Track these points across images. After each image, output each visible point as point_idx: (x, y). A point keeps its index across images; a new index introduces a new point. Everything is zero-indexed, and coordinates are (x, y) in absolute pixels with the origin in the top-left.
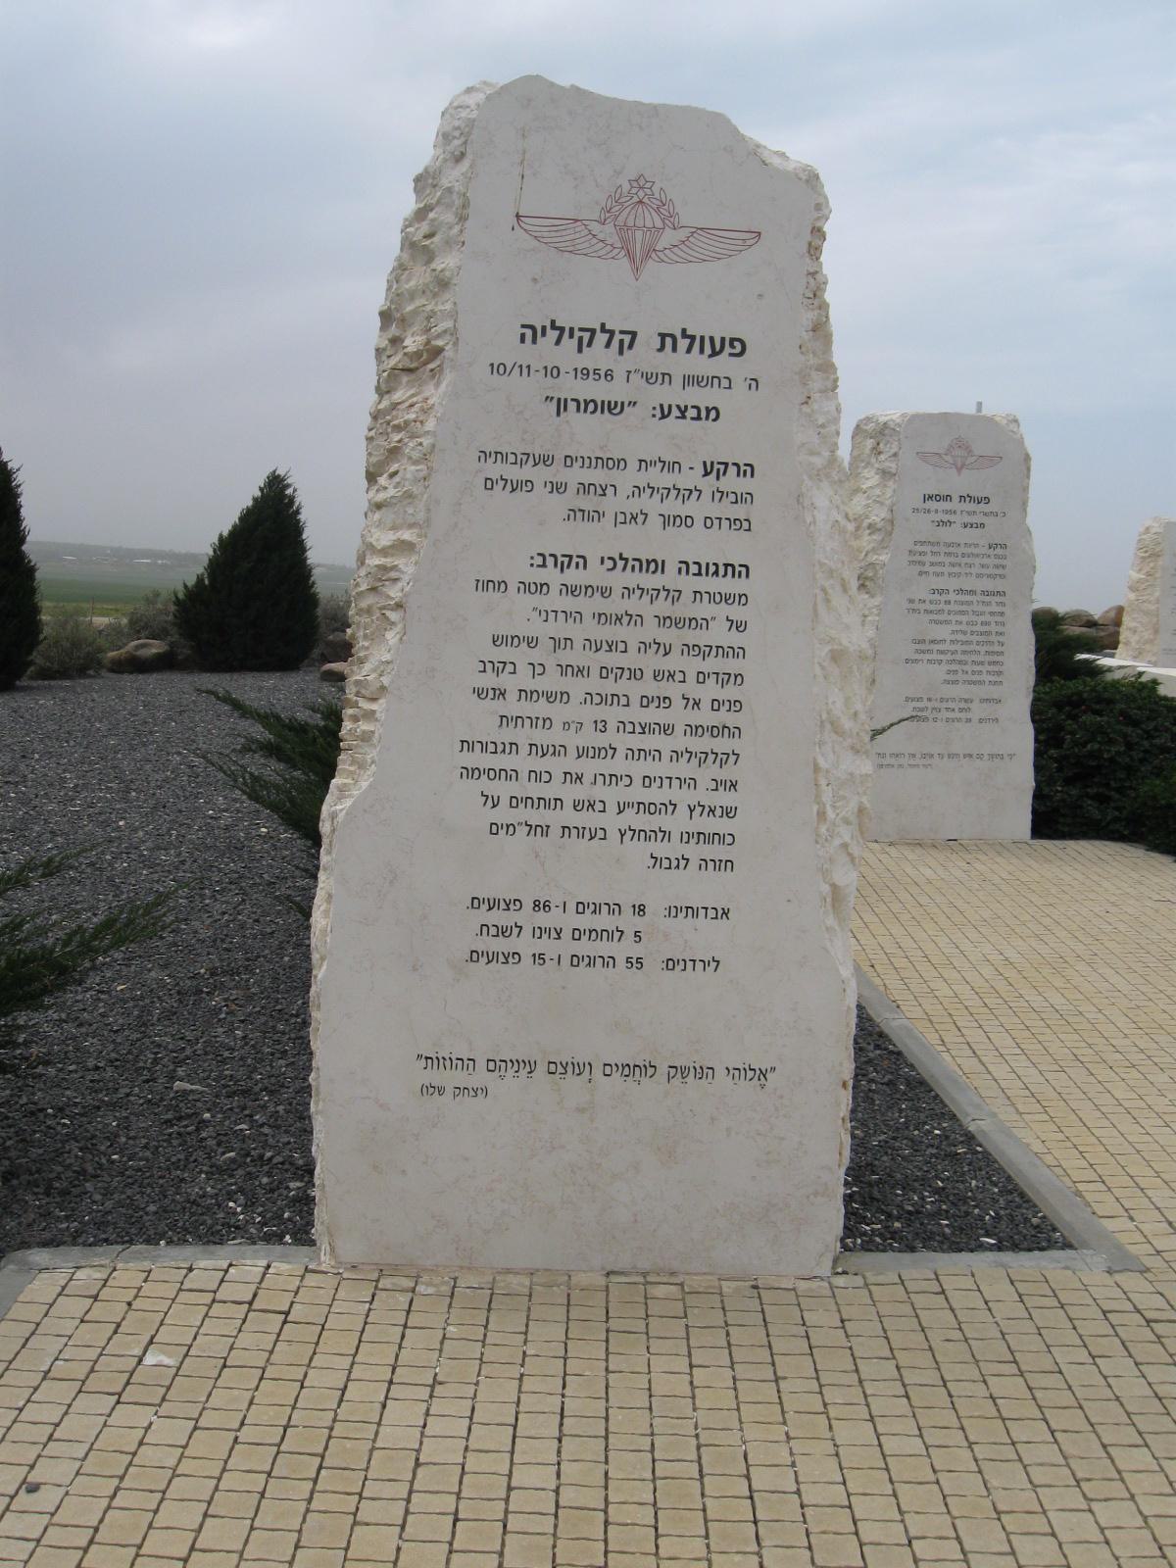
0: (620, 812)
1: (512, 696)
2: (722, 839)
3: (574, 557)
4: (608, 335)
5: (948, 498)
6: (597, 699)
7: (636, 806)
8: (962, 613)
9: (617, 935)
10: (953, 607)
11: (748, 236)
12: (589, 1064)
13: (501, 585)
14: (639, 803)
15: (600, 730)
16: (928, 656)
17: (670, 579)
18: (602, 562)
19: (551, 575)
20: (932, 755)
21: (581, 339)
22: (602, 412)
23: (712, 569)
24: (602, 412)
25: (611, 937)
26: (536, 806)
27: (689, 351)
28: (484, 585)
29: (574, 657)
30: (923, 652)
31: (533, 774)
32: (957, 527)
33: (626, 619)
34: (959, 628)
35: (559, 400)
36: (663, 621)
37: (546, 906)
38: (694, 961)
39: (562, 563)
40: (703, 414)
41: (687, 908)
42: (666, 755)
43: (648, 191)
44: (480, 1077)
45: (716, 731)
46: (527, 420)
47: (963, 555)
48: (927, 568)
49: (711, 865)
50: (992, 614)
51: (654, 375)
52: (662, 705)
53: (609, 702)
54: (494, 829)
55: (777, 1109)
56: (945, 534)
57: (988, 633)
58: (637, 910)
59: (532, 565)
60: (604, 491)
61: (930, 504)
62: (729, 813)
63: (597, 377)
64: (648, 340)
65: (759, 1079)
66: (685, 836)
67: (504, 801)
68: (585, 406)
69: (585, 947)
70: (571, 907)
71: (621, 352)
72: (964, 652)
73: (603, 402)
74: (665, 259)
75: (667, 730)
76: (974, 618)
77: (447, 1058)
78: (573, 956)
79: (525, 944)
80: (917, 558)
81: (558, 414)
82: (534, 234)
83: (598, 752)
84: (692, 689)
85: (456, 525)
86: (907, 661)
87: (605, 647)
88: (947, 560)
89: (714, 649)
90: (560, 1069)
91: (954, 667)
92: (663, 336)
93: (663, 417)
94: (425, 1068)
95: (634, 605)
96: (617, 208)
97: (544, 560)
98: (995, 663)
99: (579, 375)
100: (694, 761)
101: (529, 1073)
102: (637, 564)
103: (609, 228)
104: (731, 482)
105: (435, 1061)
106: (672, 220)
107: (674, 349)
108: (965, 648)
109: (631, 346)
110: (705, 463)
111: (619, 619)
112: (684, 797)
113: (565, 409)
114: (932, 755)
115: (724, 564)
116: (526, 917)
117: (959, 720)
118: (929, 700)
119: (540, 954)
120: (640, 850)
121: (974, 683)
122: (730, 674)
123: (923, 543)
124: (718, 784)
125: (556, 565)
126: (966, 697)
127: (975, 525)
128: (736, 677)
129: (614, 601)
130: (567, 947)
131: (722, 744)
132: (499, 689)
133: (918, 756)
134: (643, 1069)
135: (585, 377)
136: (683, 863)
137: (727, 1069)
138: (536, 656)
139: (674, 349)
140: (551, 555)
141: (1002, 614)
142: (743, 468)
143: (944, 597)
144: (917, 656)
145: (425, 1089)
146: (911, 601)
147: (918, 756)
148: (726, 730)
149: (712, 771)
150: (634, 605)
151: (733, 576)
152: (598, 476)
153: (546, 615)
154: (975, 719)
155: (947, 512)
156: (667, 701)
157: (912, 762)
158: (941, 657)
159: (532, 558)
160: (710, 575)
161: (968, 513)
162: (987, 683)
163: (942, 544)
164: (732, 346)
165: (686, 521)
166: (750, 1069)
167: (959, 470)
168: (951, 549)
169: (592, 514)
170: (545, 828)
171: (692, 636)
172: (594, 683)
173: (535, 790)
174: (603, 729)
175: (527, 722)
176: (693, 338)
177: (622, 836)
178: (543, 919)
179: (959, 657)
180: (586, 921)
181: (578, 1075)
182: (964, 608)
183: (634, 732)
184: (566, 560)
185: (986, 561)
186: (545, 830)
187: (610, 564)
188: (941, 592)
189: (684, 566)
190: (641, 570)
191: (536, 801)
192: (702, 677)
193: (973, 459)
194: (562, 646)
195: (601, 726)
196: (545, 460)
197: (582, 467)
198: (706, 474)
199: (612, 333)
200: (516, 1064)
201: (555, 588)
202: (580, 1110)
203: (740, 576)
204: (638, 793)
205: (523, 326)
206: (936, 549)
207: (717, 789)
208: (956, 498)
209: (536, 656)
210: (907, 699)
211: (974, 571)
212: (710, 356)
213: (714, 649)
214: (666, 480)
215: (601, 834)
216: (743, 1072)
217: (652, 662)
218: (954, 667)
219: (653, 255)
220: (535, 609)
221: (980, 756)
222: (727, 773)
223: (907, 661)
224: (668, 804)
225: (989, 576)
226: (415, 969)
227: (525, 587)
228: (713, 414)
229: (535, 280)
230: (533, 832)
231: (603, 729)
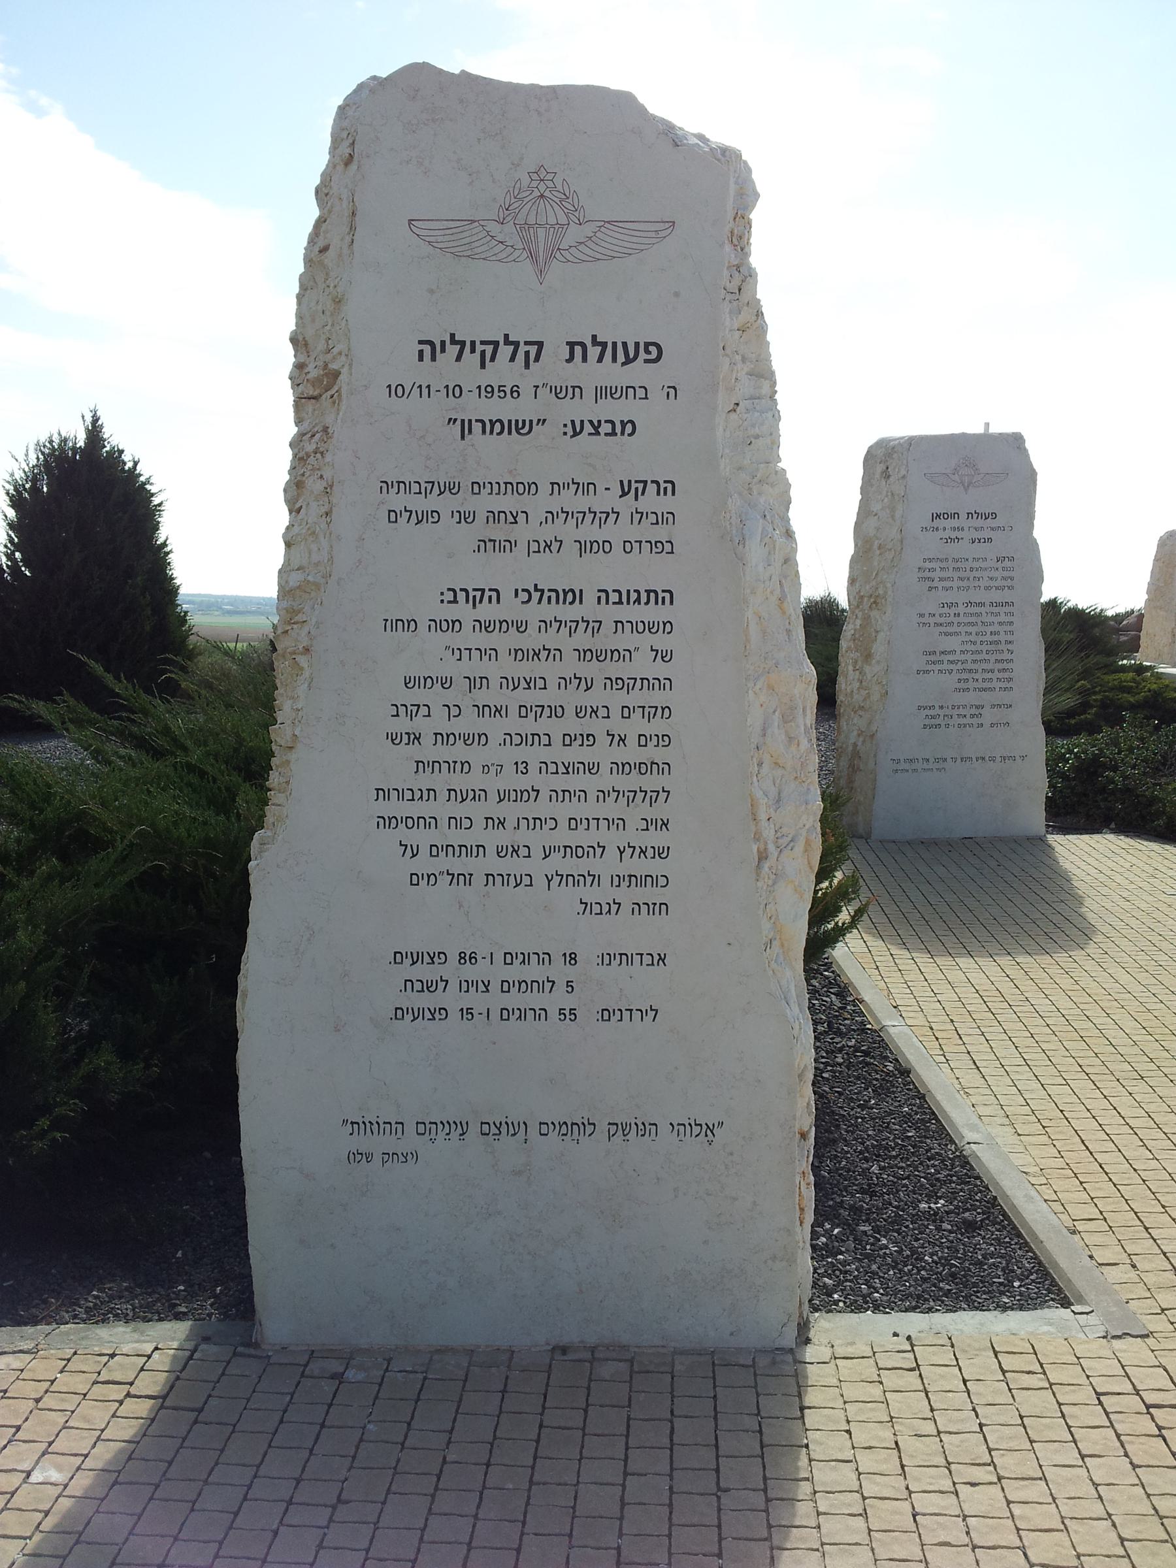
0: (546, 857)
1: (427, 740)
2: (655, 881)
4: (513, 347)
5: (955, 515)
6: (517, 739)
7: (562, 849)
9: (548, 986)
10: (962, 619)
11: (662, 226)
12: (524, 1123)
13: (410, 624)
14: (565, 847)
15: (522, 772)
16: (938, 667)
17: (588, 609)
18: (516, 595)
19: (463, 611)
20: (946, 759)
21: (483, 353)
22: (510, 433)
23: (634, 596)
24: (510, 433)
25: (541, 989)
26: (457, 853)
27: (600, 360)
28: (392, 624)
29: (491, 696)
30: (934, 663)
31: (453, 821)
33: (544, 654)
34: (968, 638)
35: (463, 421)
36: (583, 654)
37: (473, 958)
38: (631, 1010)
39: (474, 597)
40: (618, 429)
41: (621, 954)
42: (592, 797)
43: (550, 184)
44: (410, 1141)
45: (643, 768)
46: (430, 445)
47: (972, 569)
48: (935, 584)
49: (644, 908)
50: (1000, 623)
51: (564, 389)
52: (586, 742)
53: (530, 742)
54: (414, 879)
55: (726, 1167)
56: (954, 550)
57: (998, 642)
58: (568, 959)
59: (442, 601)
60: (515, 518)
61: (937, 523)
62: (661, 853)
63: (502, 394)
64: (556, 350)
65: (706, 1136)
66: (616, 879)
67: (424, 851)
68: (491, 426)
69: (515, 1000)
70: (498, 958)
71: (527, 366)
72: (974, 661)
73: (510, 421)
74: (571, 258)
75: (591, 769)
76: (983, 629)
77: (374, 1123)
78: (502, 1009)
79: (452, 999)
80: (927, 574)
81: (463, 437)
82: (427, 239)
83: (520, 795)
84: (617, 724)
85: (360, 561)
86: (918, 672)
87: (523, 684)
88: (956, 575)
89: (639, 682)
90: (494, 1130)
91: (965, 676)
92: (572, 345)
93: (575, 434)
94: (351, 1134)
95: (550, 639)
96: (516, 205)
97: (455, 596)
99: (483, 393)
100: (623, 801)
101: (461, 1135)
102: (553, 595)
103: (509, 227)
104: (650, 501)
105: (362, 1126)
106: (576, 214)
107: (585, 359)
109: (537, 359)
110: (621, 482)
111: (537, 654)
112: (612, 838)
113: (470, 431)
114: (946, 759)
115: (646, 591)
116: (451, 970)
117: (971, 725)
118: (941, 707)
119: (467, 1009)
120: (568, 896)
121: (984, 690)
122: (657, 708)
123: (930, 560)
124: (648, 824)
126: (977, 704)
127: (983, 540)
128: (663, 709)
129: (530, 636)
130: (496, 1000)
131: (652, 782)
132: (414, 734)
134: (582, 1127)
135: (489, 395)
136: (614, 908)
137: (671, 1124)
138: (451, 696)
139: (585, 359)
140: (461, 590)
142: (663, 486)
143: (953, 610)
144: (929, 667)
145: (352, 1156)
146: (922, 615)
147: (931, 760)
148: (655, 766)
149: (645, 810)
150: (550, 639)
151: (657, 603)
152: (507, 503)
153: (459, 653)
154: (987, 724)
155: (954, 529)
156: (591, 738)
157: (926, 766)
158: (951, 667)
160: (632, 603)
164: (648, 352)
165: (605, 546)
166: (696, 1125)
167: (966, 490)
168: (959, 565)
169: (503, 543)
170: (468, 877)
171: (614, 669)
172: (513, 723)
173: (456, 837)
174: (525, 771)
175: (445, 766)
176: (604, 345)
177: (549, 881)
178: (470, 972)
179: (969, 666)
180: (515, 972)
181: (512, 1135)
182: (973, 619)
183: (557, 773)
184: (478, 594)
186: (468, 879)
187: (525, 596)
188: (950, 605)
189: (603, 595)
190: (557, 602)
191: (457, 849)
192: (626, 712)
194: (478, 685)
195: (522, 767)
196: (451, 488)
197: (491, 493)
198: (624, 494)
199: (516, 344)
200: (447, 1126)
201: (468, 625)
202: (518, 1173)
203: (663, 603)
204: (563, 836)
205: (421, 342)
206: (944, 565)
207: (647, 829)
208: (963, 516)
209: (451, 696)
210: (920, 708)
211: (982, 583)
212: (623, 364)
213: (639, 682)
214: (582, 502)
215: (526, 880)
216: (688, 1127)
217: (572, 698)
218: (965, 676)
219: (558, 255)
220: (447, 648)
221: (993, 759)
222: (659, 811)
223: (918, 672)
224: (596, 846)
226: (337, 1030)
227: (436, 625)
228: (629, 428)
229: (431, 291)
230: (455, 880)
231: (525, 771)
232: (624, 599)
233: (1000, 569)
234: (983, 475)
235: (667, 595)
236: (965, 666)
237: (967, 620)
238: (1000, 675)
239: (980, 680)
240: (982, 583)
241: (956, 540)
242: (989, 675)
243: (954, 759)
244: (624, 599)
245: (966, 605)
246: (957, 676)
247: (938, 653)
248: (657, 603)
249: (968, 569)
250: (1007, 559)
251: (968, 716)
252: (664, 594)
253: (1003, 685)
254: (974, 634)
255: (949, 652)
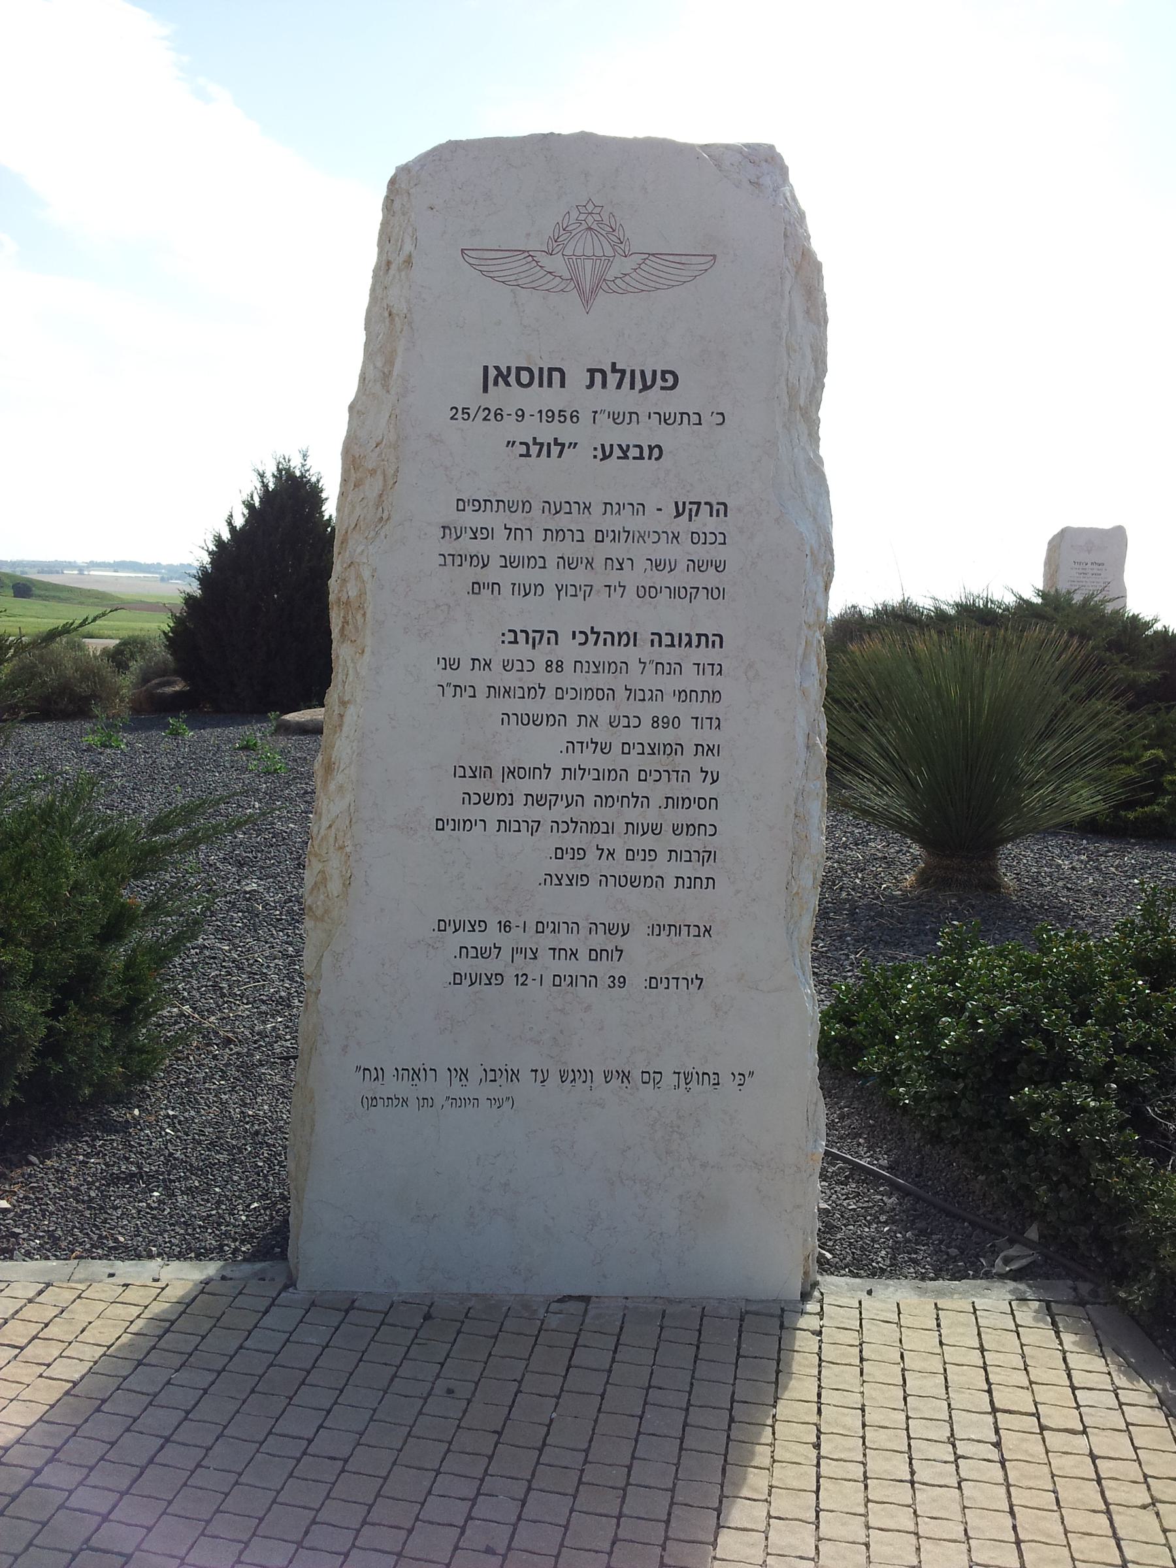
5: (554, 376)
8: (597, 693)
10: (570, 679)
16: (494, 812)
20: (516, 1074)
30: (485, 800)
32: (581, 459)
34: (585, 734)
47: (600, 536)
48: (493, 573)
50: (683, 695)
61: (499, 396)
72: (604, 800)
76: (633, 708)
80: (467, 545)
86: (440, 824)
88: (553, 550)
91: (574, 840)
98: (693, 828)
108: (607, 788)
114: (516, 1074)
117: (591, 980)
118: (505, 926)
121: (632, 882)
123: (480, 505)
133: (475, 1074)
141: (714, 695)
143: (542, 654)
146: (451, 664)
147: (475, 1074)
154: (637, 981)
155: (550, 416)
157: (458, 1090)
158: (536, 812)
161: (614, 417)
162: (670, 882)
163: (537, 506)
167: (587, 299)
168: (563, 521)
179: (589, 812)
182: (602, 680)
185: (666, 550)
188: (535, 638)
193: (629, 264)
206: (517, 520)
208: (577, 377)
210: (442, 925)
211: (632, 578)
218: (574, 840)
221: (653, 1077)
223: (440, 824)
225: (674, 593)
233: (685, 538)
234: (638, 258)
236: (575, 812)
237: (581, 681)
238: (681, 842)
239: (620, 854)
240: (632, 578)
241: (555, 450)
242: (649, 841)
243: (539, 1073)
245: (582, 638)
246: (549, 840)
247: (498, 774)
249: (589, 536)
250: (705, 509)
251: (583, 954)
253: (686, 870)
254: (603, 721)
255: (532, 772)
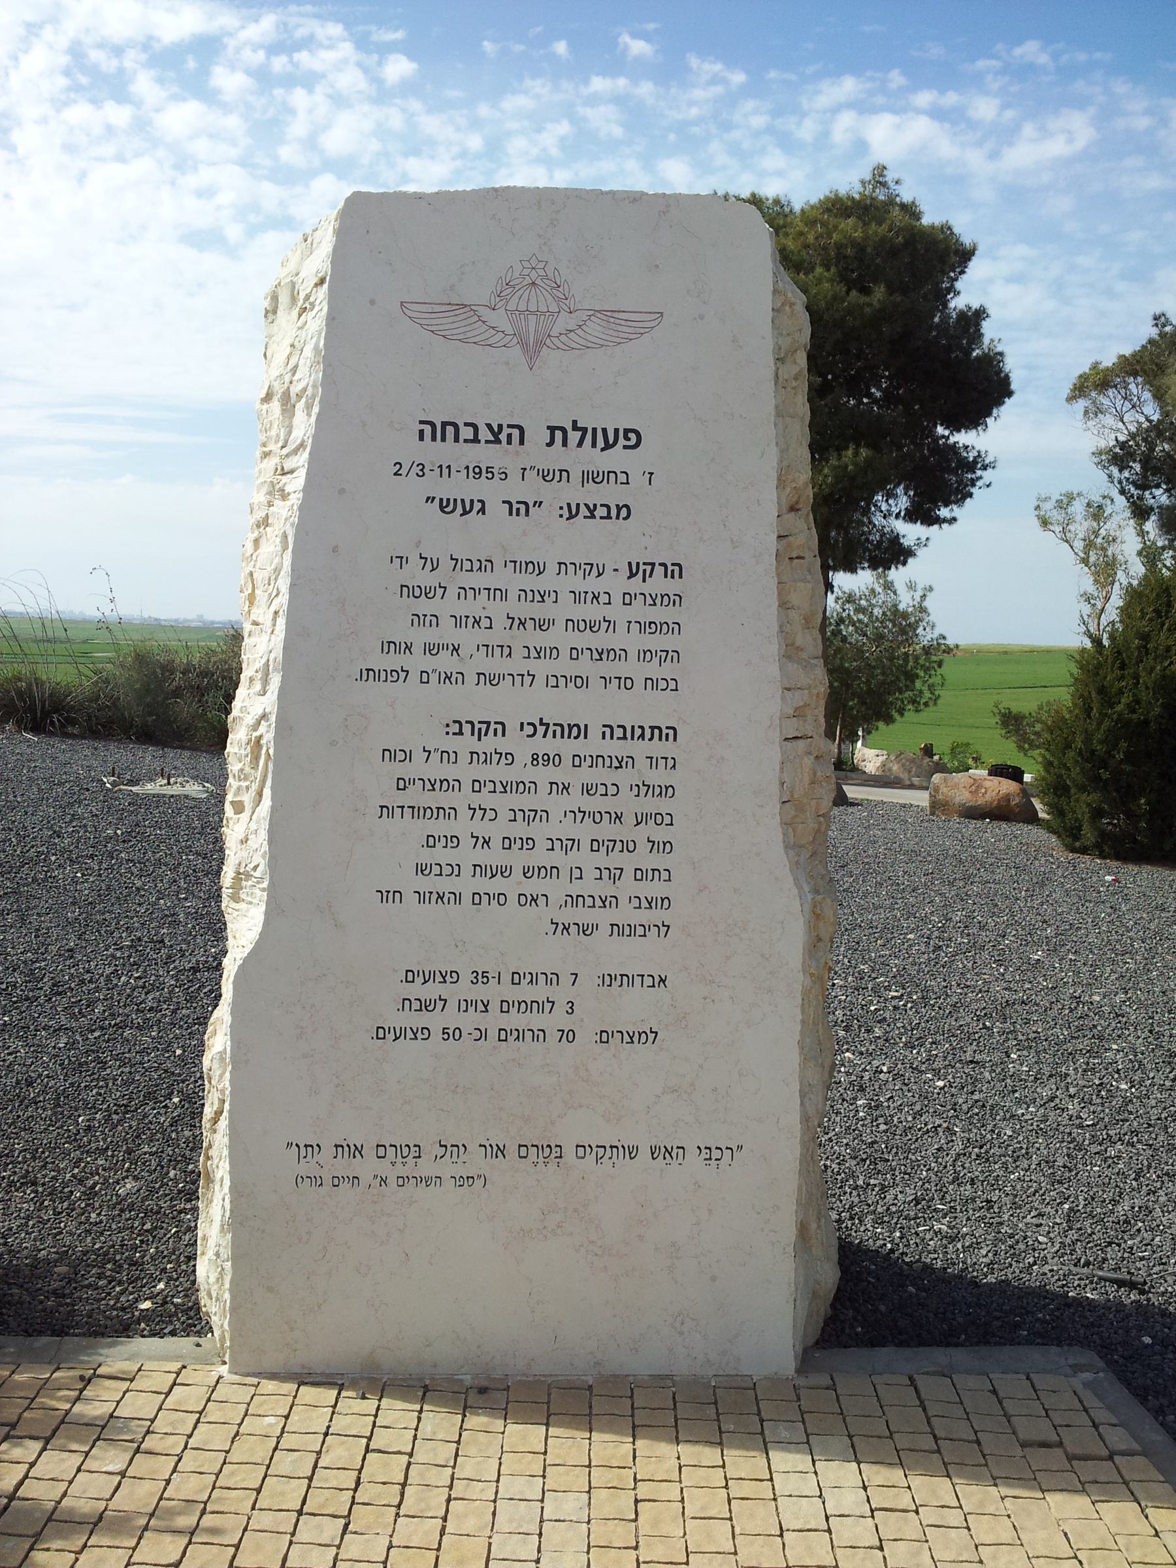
3: (492, 723)
18: (522, 729)
23: (638, 732)
27: (580, 444)
39: (480, 729)
51: (551, 472)
59: (447, 733)
102: (558, 729)
115: (650, 727)
125: (473, 734)
151: (660, 739)
159: (448, 725)
164: (627, 438)
184: (484, 727)
187: (530, 730)
189: (608, 730)
190: (562, 737)
203: (667, 739)
212: (602, 450)
232: (629, 735)
235: (671, 732)
244: (629, 735)
248: (660, 739)
252: (668, 731)
